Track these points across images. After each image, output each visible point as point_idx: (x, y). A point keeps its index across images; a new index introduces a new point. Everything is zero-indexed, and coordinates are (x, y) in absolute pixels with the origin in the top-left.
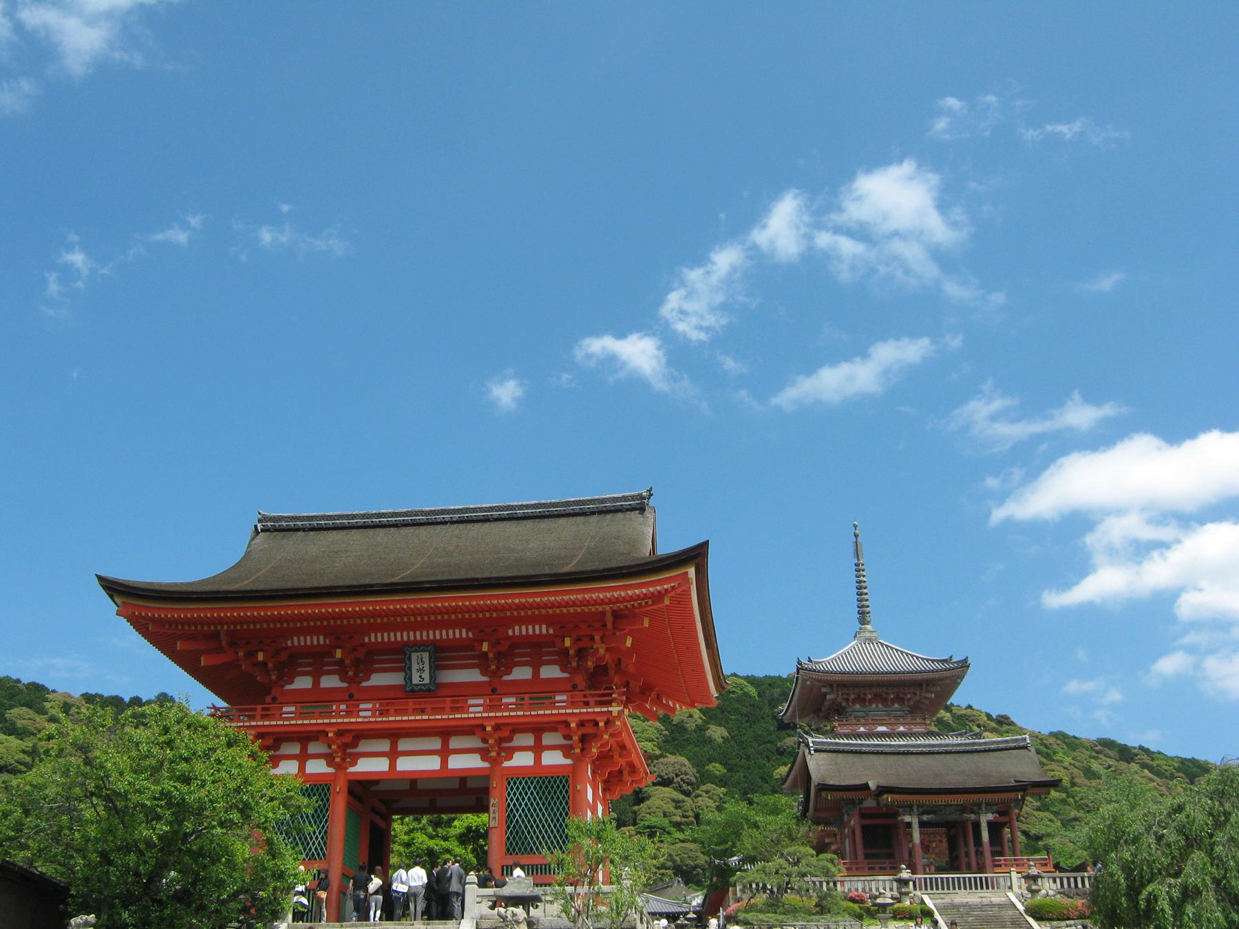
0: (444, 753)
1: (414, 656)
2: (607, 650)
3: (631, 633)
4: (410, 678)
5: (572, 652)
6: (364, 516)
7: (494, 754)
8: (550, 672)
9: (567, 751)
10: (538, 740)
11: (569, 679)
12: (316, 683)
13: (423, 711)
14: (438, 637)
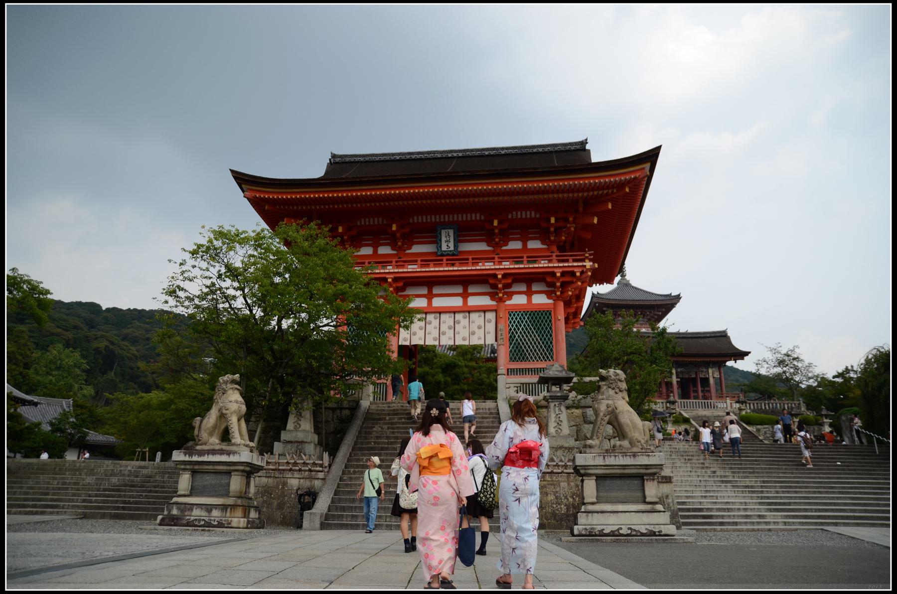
0: (465, 295)
1: (443, 232)
2: (575, 228)
3: (594, 215)
4: (441, 247)
5: (552, 229)
6: (399, 154)
7: (501, 295)
8: (534, 244)
9: (549, 295)
10: (529, 287)
11: (548, 249)
12: (375, 251)
13: (453, 265)
14: (460, 219)
